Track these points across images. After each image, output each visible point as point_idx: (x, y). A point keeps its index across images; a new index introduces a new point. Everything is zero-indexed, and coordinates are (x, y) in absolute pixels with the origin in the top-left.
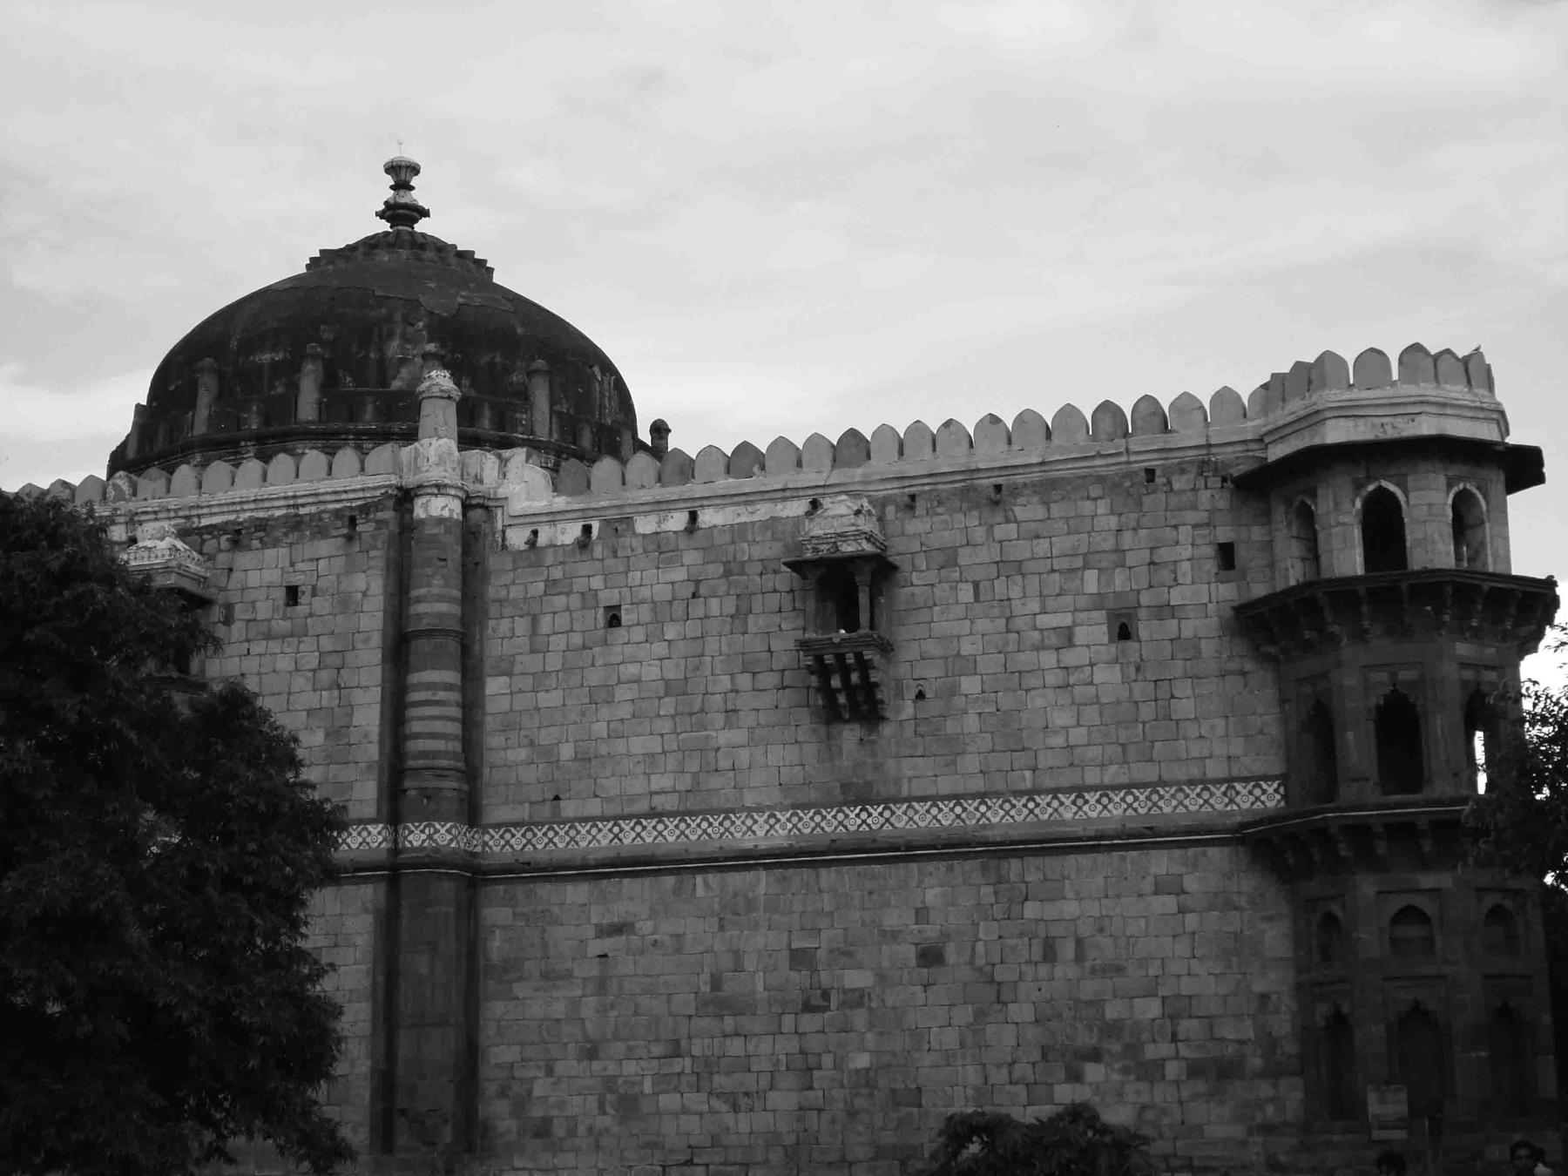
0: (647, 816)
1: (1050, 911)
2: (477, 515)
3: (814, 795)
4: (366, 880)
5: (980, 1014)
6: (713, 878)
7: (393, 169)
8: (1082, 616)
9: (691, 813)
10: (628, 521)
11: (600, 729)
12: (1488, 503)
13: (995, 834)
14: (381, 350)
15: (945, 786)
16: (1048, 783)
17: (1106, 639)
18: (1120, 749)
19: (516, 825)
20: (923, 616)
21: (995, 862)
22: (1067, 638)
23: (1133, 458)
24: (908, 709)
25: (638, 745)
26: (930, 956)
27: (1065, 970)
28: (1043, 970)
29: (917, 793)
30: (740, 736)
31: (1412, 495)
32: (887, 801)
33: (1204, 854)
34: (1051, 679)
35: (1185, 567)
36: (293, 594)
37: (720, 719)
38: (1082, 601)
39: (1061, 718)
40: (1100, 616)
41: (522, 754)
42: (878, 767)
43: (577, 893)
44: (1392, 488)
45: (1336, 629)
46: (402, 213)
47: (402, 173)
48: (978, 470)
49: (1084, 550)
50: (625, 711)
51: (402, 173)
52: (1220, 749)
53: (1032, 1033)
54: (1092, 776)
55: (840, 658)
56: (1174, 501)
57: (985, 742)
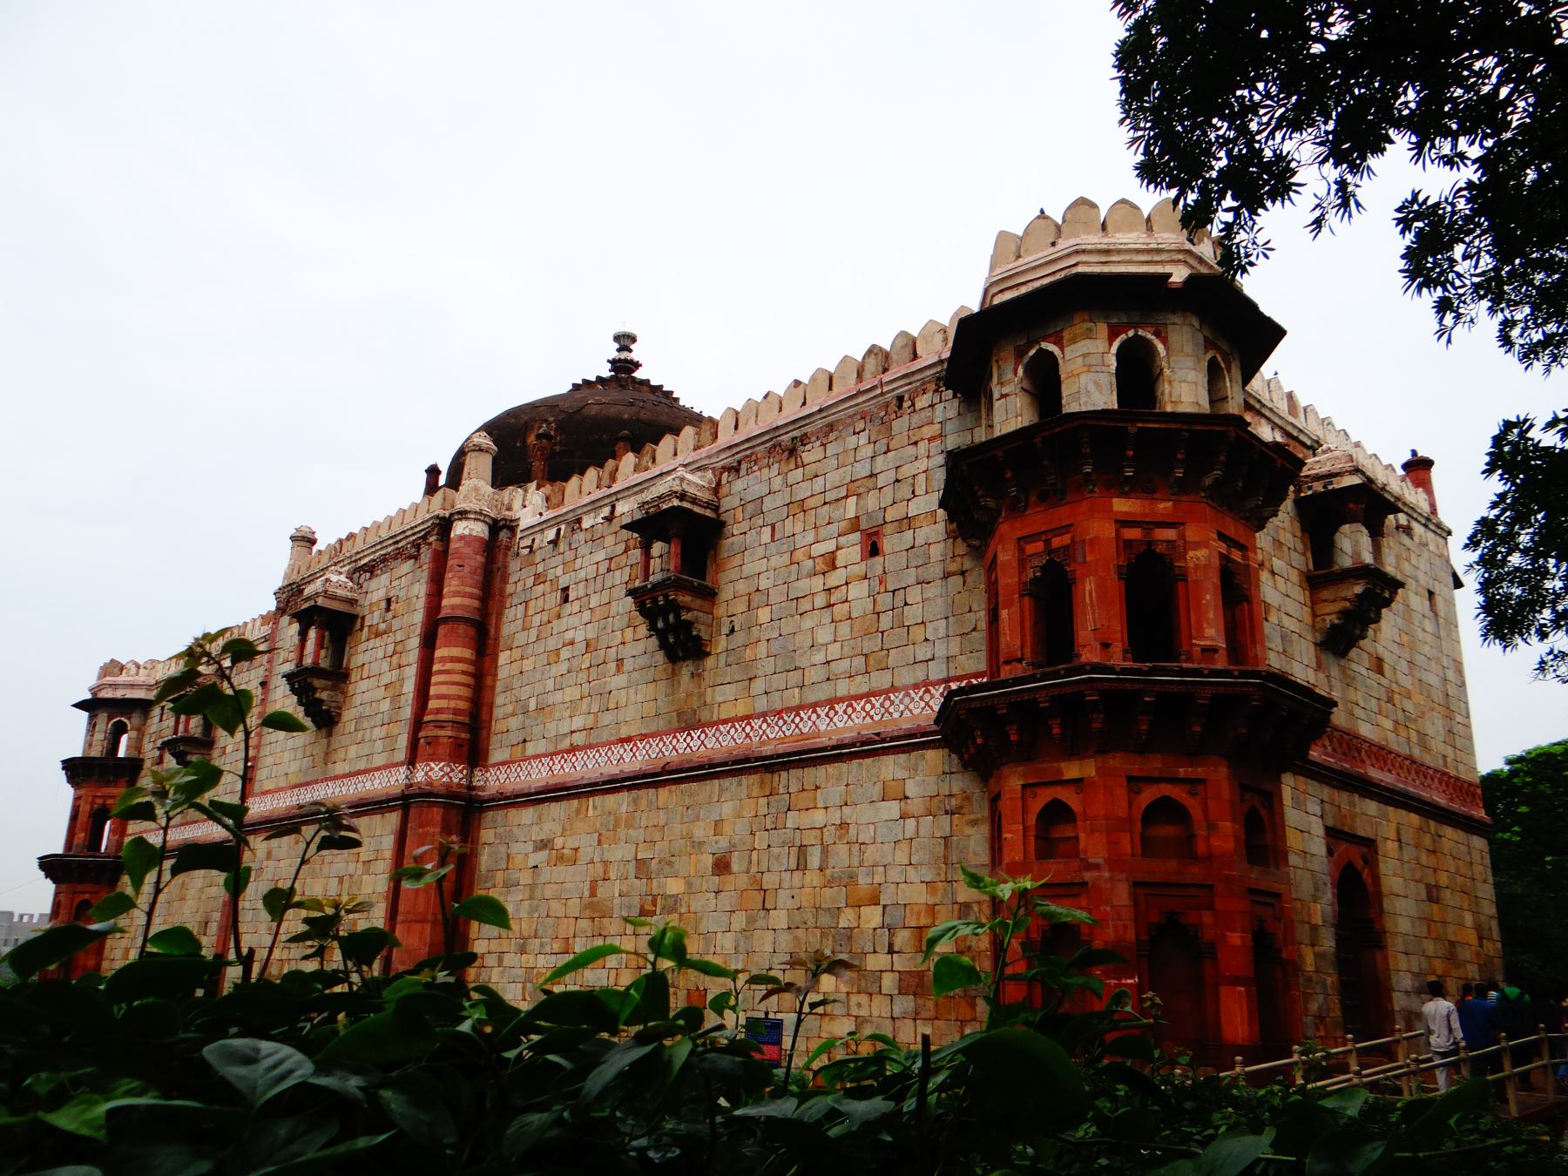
0: (568, 752)
1: (806, 819)
2: (504, 535)
3: (661, 724)
4: (391, 809)
5: (751, 921)
6: (598, 799)
7: (617, 338)
8: (842, 540)
9: (590, 747)
10: (579, 521)
11: (550, 685)
12: (1167, 348)
13: (768, 750)
14: (524, 441)
15: (741, 710)
16: (811, 697)
17: (858, 558)
18: (863, 659)
19: (503, 764)
20: (737, 561)
21: (768, 776)
22: (831, 562)
23: (886, 389)
24: (722, 644)
25: (571, 693)
26: (722, 866)
27: (813, 878)
28: (797, 874)
29: (723, 717)
30: (621, 680)
31: (1067, 350)
32: (700, 725)
33: (923, 757)
34: (820, 601)
35: (922, 477)
36: (389, 601)
37: (613, 666)
38: (844, 524)
39: (824, 636)
40: (856, 537)
41: (510, 709)
42: (702, 695)
43: (527, 815)
44: (1051, 347)
45: (991, 503)
46: (624, 368)
47: (625, 341)
48: (777, 428)
49: (848, 479)
50: (563, 667)
51: (625, 341)
52: (941, 651)
53: (785, 942)
54: (843, 688)
55: (655, 601)
56: (916, 419)
57: (769, 665)
